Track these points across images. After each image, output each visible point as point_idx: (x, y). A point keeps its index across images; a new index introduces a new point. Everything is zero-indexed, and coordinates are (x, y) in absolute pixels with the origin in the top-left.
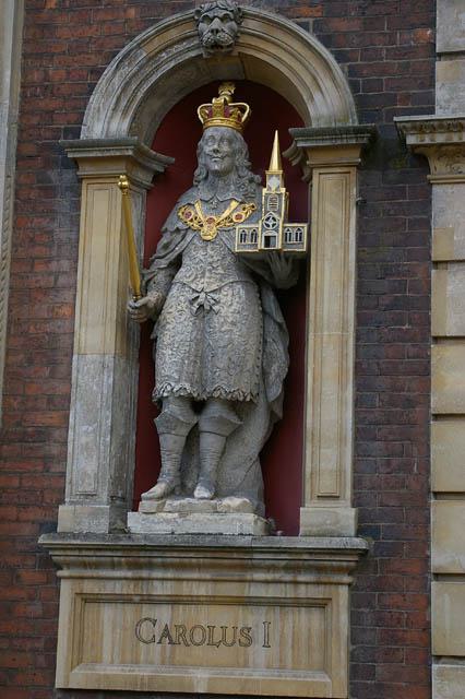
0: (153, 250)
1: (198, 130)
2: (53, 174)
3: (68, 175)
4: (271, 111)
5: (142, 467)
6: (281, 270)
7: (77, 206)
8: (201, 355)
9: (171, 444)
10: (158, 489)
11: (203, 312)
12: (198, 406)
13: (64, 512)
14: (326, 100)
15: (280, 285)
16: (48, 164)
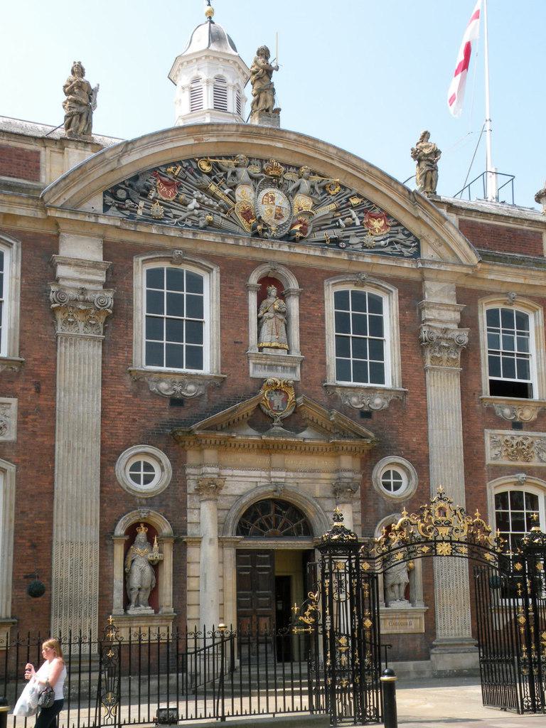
1: (136, 534)
2: (107, 541)
3: (111, 542)
4: (152, 532)
5: (127, 602)
6: (156, 562)
7: (113, 548)
8: (142, 579)
9: (133, 599)
10: (133, 605)
11: (142, 571)
12: (139, 589)
13: (114, 610)
14: (166, 529)
15: (156, 566)
16: (106, 539)
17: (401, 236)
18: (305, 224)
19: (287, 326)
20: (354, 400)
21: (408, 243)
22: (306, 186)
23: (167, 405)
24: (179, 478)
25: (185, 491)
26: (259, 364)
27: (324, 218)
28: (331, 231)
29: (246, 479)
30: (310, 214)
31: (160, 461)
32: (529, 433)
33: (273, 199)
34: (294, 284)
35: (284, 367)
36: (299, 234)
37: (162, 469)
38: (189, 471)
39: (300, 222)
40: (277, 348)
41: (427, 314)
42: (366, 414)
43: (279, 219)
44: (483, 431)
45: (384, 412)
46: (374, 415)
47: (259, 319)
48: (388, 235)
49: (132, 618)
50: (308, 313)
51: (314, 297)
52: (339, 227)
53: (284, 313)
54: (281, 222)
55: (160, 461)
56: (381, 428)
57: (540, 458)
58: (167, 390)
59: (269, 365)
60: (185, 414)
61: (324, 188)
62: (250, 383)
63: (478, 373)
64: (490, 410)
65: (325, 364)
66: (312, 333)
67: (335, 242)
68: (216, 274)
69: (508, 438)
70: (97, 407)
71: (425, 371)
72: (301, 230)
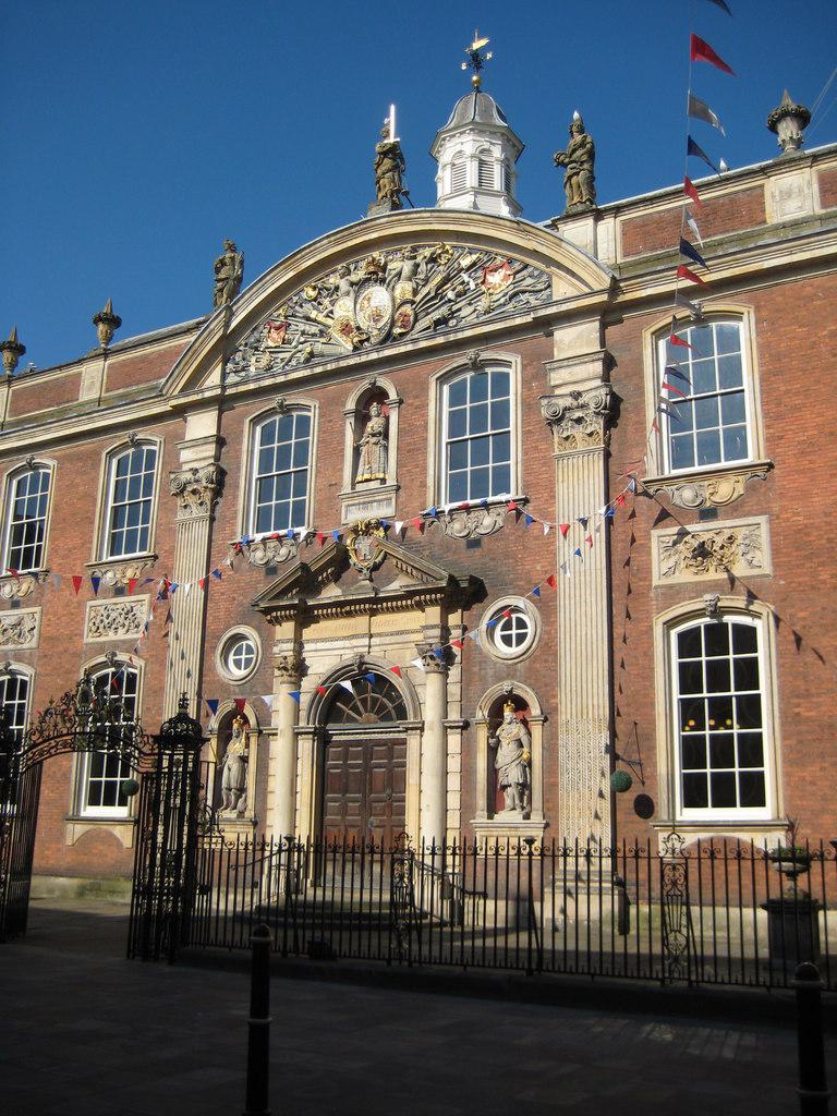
0: (221, 754)
1: (232, 725)
17: (529, 281)
19: (386, 448)
22: (407, 267)
26: (354, 505)
27: (429, 299)
29: (329, 649)
32: (729, 523)
34: (393, 396)
35: (380, 501)
36: (397, 331)
40: (367, 480)
42: (474, 543)
44: (649, 534)
45: (495, 532)
46: (485, 539)
48: (512, 286)
50: (410, 425)
51: (417, 402)
52: (450, 301)
53: (380, 433)
54: (380, 325)
56: (493, 559)
58: (262, 559)
59: (364, 503)
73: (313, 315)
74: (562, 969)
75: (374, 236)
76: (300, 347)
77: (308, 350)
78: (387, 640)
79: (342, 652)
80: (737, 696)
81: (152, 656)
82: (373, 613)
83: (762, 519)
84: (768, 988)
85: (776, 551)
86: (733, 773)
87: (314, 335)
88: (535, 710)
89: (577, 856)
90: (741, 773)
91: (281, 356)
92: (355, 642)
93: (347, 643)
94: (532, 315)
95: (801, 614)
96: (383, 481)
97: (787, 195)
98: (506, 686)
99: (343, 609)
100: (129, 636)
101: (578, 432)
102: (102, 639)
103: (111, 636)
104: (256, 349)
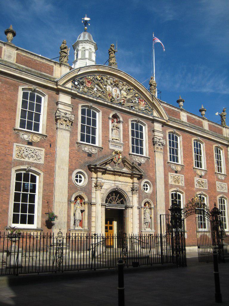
14: (86, 200)
15: (82, 211)
18: (124, 100)
20: (137, 159)
21: (149, 110)
22: (124, 89)
23: (87, 156)
24: (90, 182)
25: (91, 186)
28: (130, 103)
30: (126, 98)
31: (84, 175)
32: (179, 175)
33: (117, 91)
34: (121, 119)
37: (85, 178)
38: (93, 179)
39: (123, 99)
40: (116, 139)
41: (156, 133)
42: (140, 165)
43: (118, 97)
46: (142, 165)
47: (112, 129)
49: (76, 230)
52: (132, 102)
55: (84, 175)
57: (182, 183)
60: (91, 159)
61: (129, 90)
62: (109, 151)
63: (167, 154)
64: (170, 166)
65: (129, 146)
66: (125, 136)
67: (132, 107)
68: (101, 113)
69: (174, 176)
70: (68, 154)
71: (155, 151)
72: (124, 102)
73: (101, 85)
74: (49, 271)
75: (119, 75)
76: (96, 92)
77: (100, 94)
78: (123, 183)
79: (111, 184)
80: (29, 194)
81: (46, 171)
82: (120, 175)
83: (183, 175)
84: (38, 273)
85: (185, 182)
86: (19, 214)
87: (100, 91)
88: (153, 206)
89: (110, 238)
90: (19, 214)
91: (91, 91)
92: (116, 182)
93: (114, 182)
94: (154, 118)
95: (188, 194)
96: (120, 142)
97: (183, 116)
98: (148, 200)
99: (115, 173)
100: (35, 162)
101: (160, 147)
102: (23, 159)
103: (27, 159)
104: (82, 84)
